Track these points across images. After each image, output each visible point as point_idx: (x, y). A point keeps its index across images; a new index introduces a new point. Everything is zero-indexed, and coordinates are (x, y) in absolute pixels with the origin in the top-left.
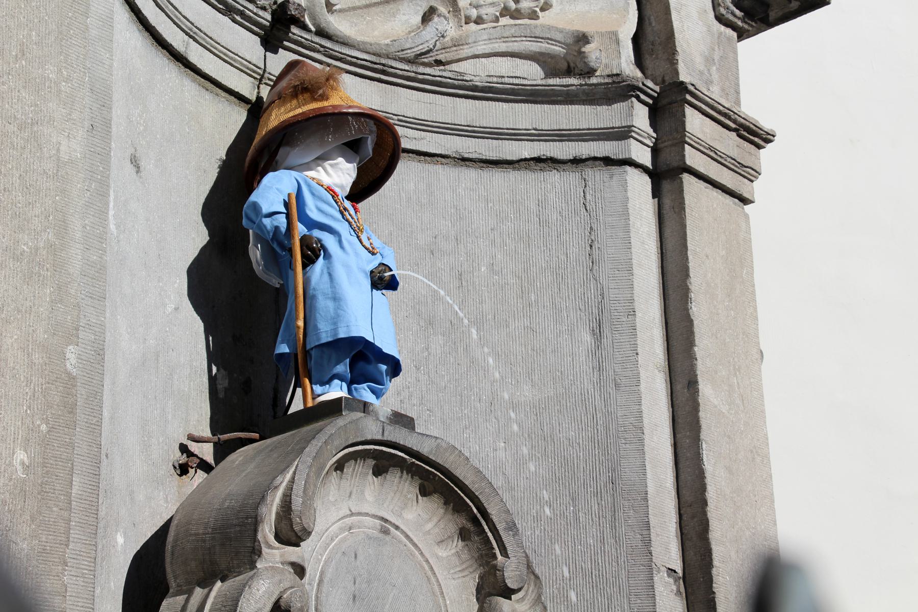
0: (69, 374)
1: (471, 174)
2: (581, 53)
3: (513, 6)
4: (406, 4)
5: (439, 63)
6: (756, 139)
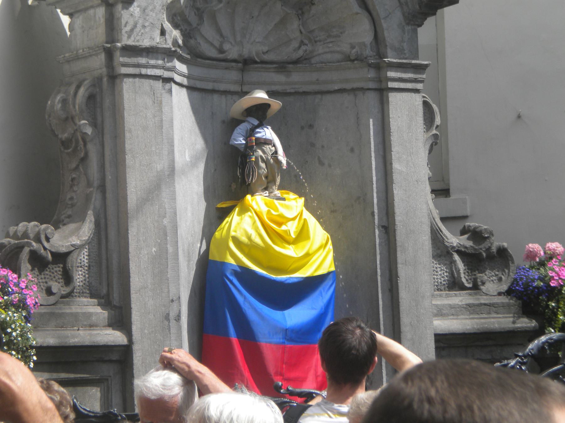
1: (319, 96)
5: (306, 59)
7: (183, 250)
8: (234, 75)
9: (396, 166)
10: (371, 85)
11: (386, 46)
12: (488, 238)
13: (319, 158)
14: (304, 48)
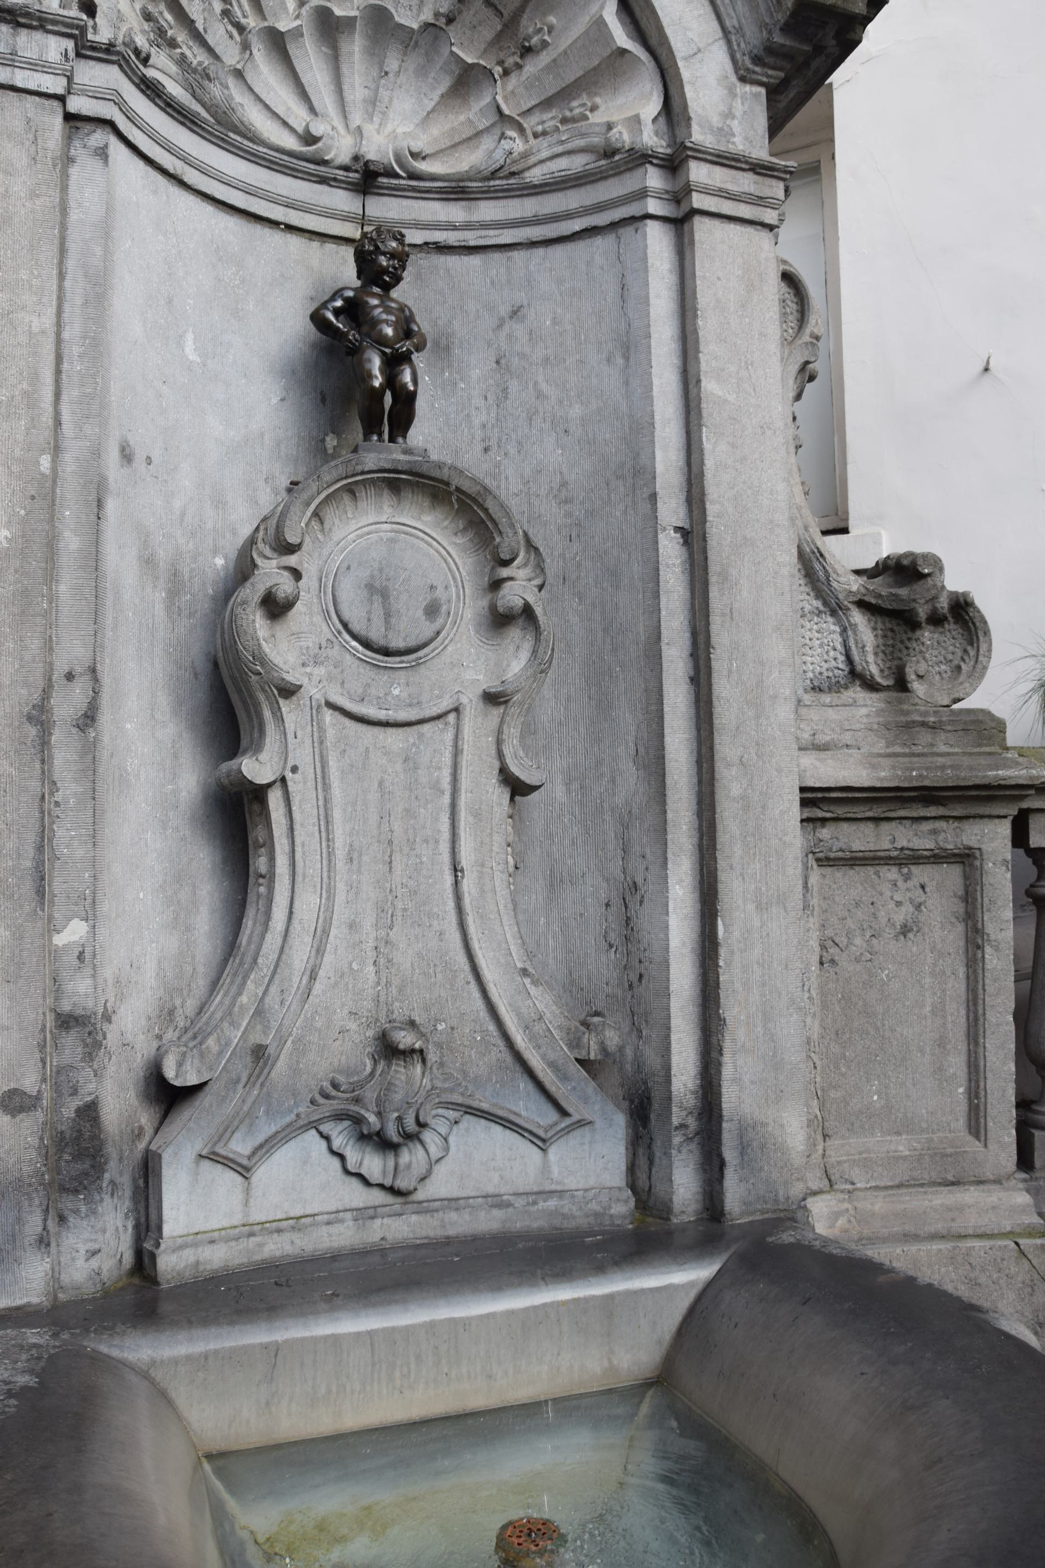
0: (43, 475)
1: (540, 251)
2: (607, 140)
3: (568, 114)
4: (485, 136)
5: (513, 174)
6: (776, 174)
7: (148, 562)
8: (342, 200)
9: (709, 386)
10: (653, 206)
11: (689, 119)
12: (929, 575)
13: (536, 383)
14: (506, 145)
